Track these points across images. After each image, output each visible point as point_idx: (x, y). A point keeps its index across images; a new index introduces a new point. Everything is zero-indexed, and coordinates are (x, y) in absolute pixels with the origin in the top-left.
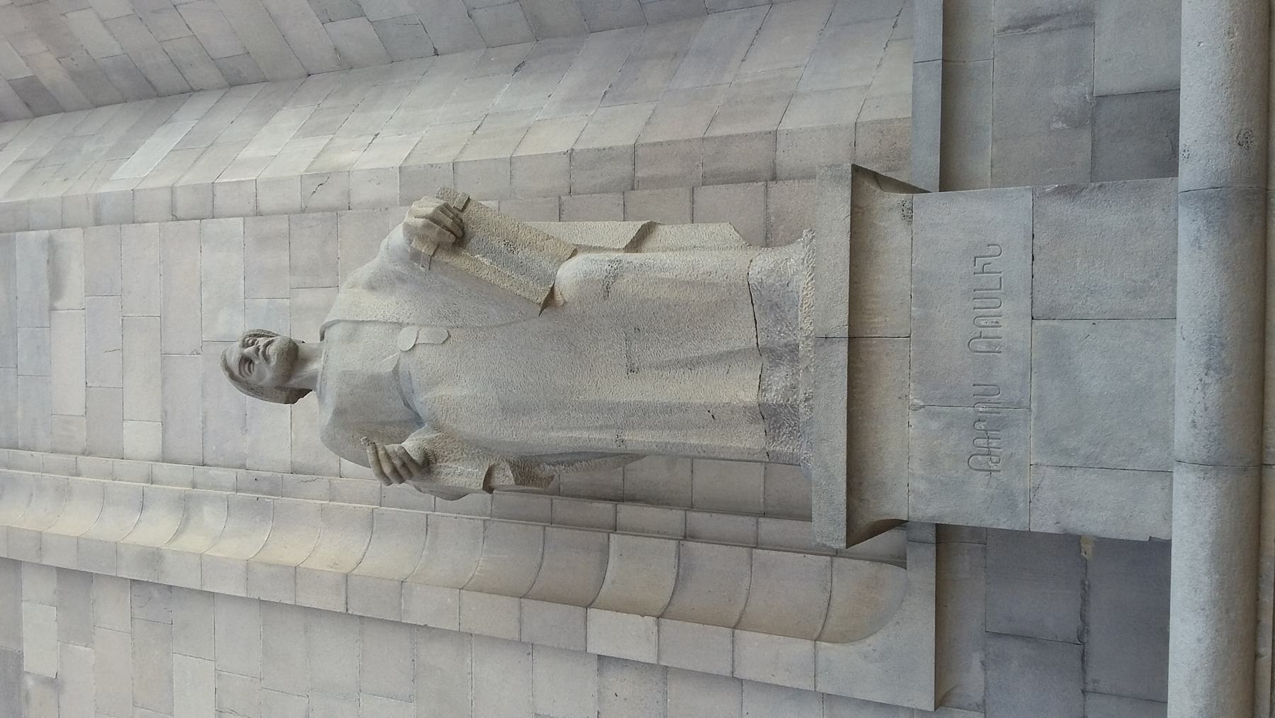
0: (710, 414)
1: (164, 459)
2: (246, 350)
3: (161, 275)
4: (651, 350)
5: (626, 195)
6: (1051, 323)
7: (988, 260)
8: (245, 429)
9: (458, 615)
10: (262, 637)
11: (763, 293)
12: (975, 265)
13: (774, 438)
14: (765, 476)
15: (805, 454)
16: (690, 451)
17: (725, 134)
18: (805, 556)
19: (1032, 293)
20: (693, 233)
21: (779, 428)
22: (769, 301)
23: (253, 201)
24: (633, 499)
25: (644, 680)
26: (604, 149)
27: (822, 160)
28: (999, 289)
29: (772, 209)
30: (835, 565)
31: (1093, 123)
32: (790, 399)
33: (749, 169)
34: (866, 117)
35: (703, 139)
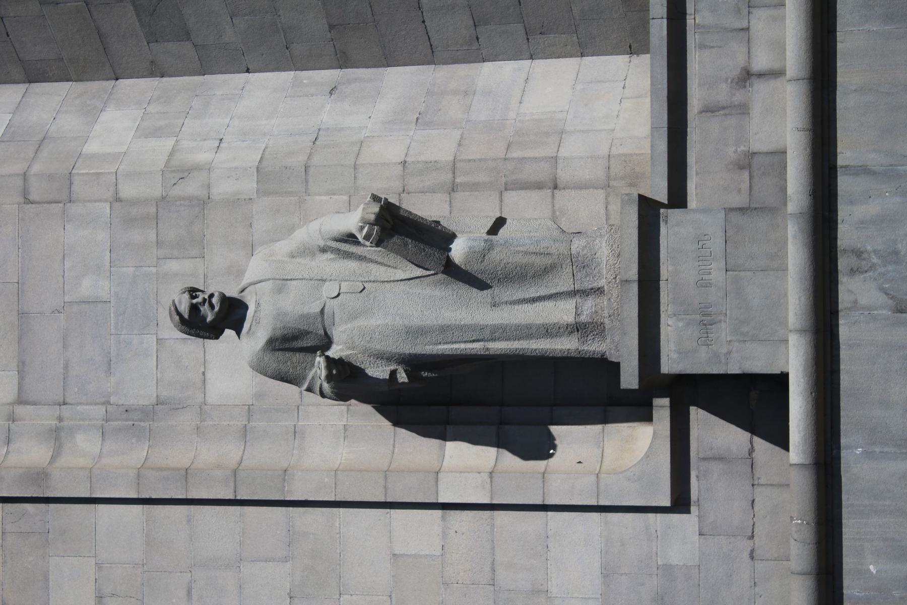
0: (545, 330)
1: (21, 401)
2: (195, 301)
3: (19, 248)
4: (507, 293)
5: (452, 194)
6: (735, 273)
7: (705, 242)
8: (109, 371)
9: (334, 489)
10: (145, 531)
13: (584, 342)
18: (585, 427)
21: (587, 336)
23: (112, 189)
25: (477, 519)
26: (431, 162)
27: (588, 177)
29: (557, 206)
30: (605, 431)
31: (750, 167)
34: (614, 151)
35: (505, 159)
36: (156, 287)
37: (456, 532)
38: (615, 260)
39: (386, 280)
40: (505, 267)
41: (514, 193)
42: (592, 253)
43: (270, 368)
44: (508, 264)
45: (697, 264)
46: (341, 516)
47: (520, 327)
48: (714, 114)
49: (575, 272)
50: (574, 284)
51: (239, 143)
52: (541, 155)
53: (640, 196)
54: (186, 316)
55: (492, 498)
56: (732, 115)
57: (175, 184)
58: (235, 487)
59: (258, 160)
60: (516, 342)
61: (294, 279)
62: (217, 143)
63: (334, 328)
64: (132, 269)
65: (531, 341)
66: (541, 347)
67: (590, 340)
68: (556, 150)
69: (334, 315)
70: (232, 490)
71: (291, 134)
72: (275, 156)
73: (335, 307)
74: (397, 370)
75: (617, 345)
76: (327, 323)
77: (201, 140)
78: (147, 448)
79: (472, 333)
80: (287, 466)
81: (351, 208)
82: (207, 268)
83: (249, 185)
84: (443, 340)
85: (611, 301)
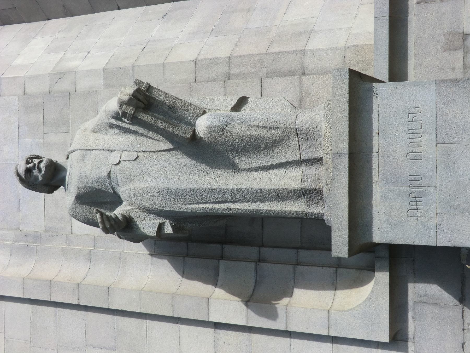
5: (226, 82)
6: (445, 145)
10: (31, 319)
12: (409, 118)
13: (309, 205)
17: (277, 51)
18: (322, 268)
19: (436, 131)
20: (266, 102)
21: (312, 200)
24: (231, 243)
28: (420, 129)
32: (318, 185)
35: (266, 54)
39: (153, 150)
40: (241, 140)
41: (270, 80)
42: (314, 127)
43: (81, 217)
44: (243, 136)
45: (407, 136)
47: (255, 192)
49: (300, 143)
50: (300, 154)
52: (292, 50)
53: (351, 71)
54: (23, 176)
55: (247, 322)
59: (105, 64)
60: (253, 204)
61: (93, 150)
63: (118, 188)
64: (30, 141)
65: (265, 203)
66: (273, 209)
68: (305, 45)
69: (117, 178)
70: (77, 299)
73: (117, 172)
74: (164, 223)
76: (114, 184)
79: (217, 196)
82: (71, 139)
83: (99, 82)
84: (195, 200)
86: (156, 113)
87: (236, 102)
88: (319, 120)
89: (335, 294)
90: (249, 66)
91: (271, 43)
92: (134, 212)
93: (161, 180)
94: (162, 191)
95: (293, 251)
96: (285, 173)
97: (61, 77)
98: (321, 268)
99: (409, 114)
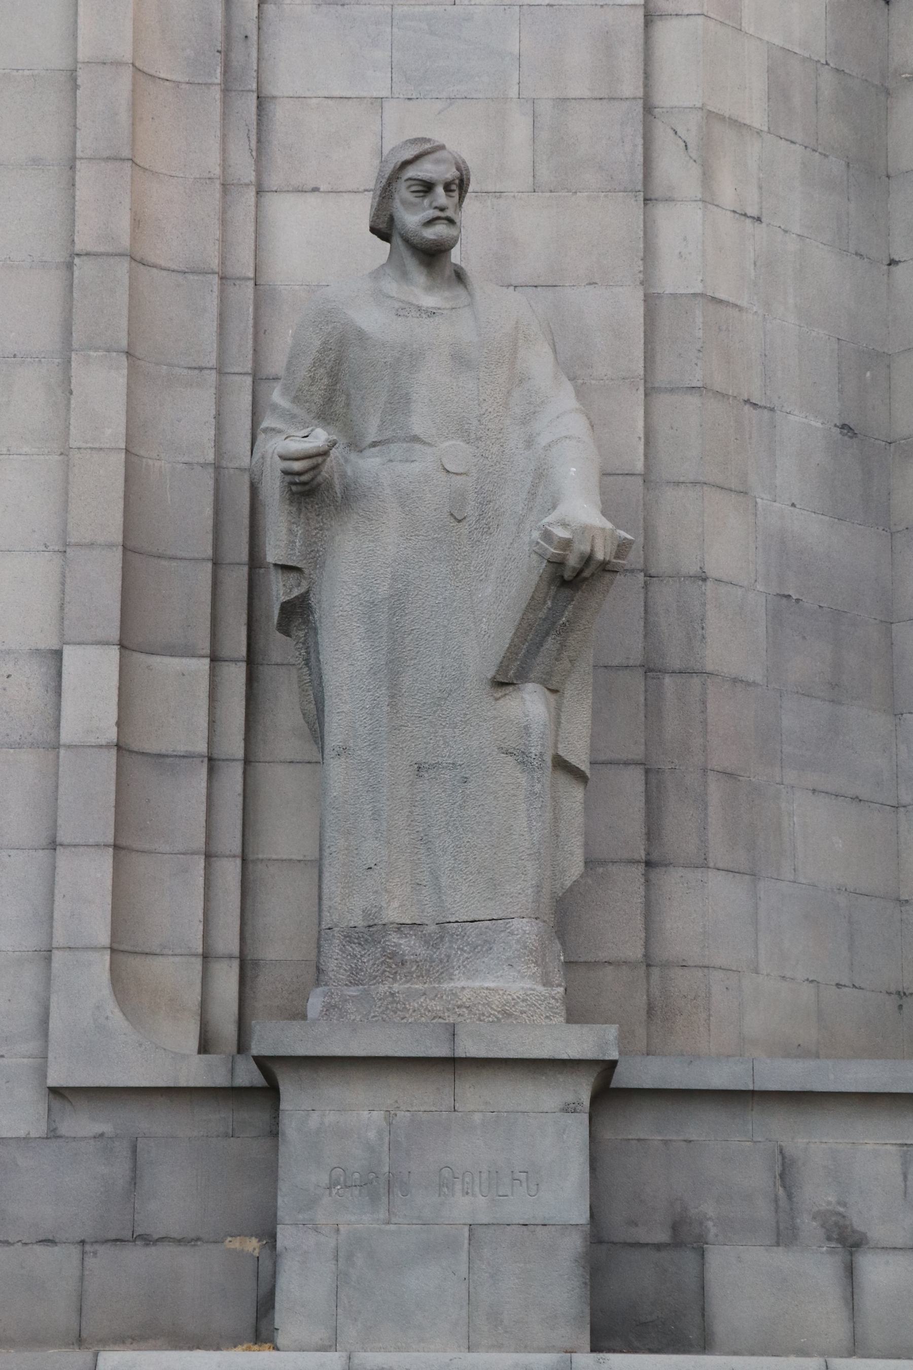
0: (372, 865)
2: (440, 190)
4: (443, 794)
6: (466, 1241)
7: (524, 1185)
9: (91, 445)
10: (14, 73)
11: (502, 934)
12: (520, 1172)
14: (290, 860)
15: (337, 994)
16: (330, 837)
20: (574, 831)
21: (360, 944)
22: (495, 940)
24: (251, 679)
25: (33, 716)
26: (703, 628)
27: (668, 926)
29: (613, 869)
30: (193, 959)
33: (664, 831)
36: (481, 96)
37: (9, 676)
38: (497, 1006)
46: (42, 457)
48: (778, 1177)
49: (480, 924)
50: (457, 922)
51: (752, 255)
56: (776, 1212)
57: (676, 133)
58: (96, 255)
59: (717, 295)
62: (752, 211)
67: (353, 949)
68: (720, 865)
70: (89, 249)
71: (765, 355)
72: (724, 328)
75: (338, 1008)
77: (759, 179)
78: (174, 78)
80: (137, 354)
81: (620, 477)
82: (514, 197)
85: (420, 998)
86: (552, 603)
87: (575, 764)
88: (524, 972)
89: (143, 953)
90: (679, 724)
91: (730, 775)
92: (328, 502)
93: (404, 588)
94: (380, 590)
95: (237, 850)
96: (418, 884)
97: (690, 150)
98: (201, 917)
99: (527, 1172)
